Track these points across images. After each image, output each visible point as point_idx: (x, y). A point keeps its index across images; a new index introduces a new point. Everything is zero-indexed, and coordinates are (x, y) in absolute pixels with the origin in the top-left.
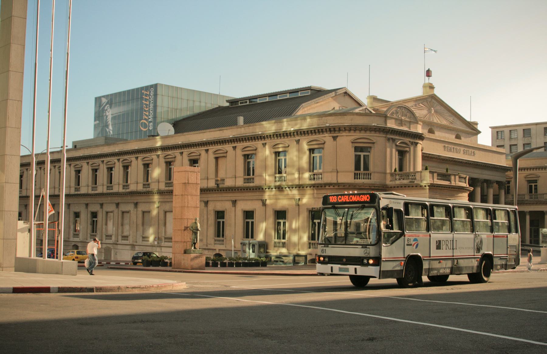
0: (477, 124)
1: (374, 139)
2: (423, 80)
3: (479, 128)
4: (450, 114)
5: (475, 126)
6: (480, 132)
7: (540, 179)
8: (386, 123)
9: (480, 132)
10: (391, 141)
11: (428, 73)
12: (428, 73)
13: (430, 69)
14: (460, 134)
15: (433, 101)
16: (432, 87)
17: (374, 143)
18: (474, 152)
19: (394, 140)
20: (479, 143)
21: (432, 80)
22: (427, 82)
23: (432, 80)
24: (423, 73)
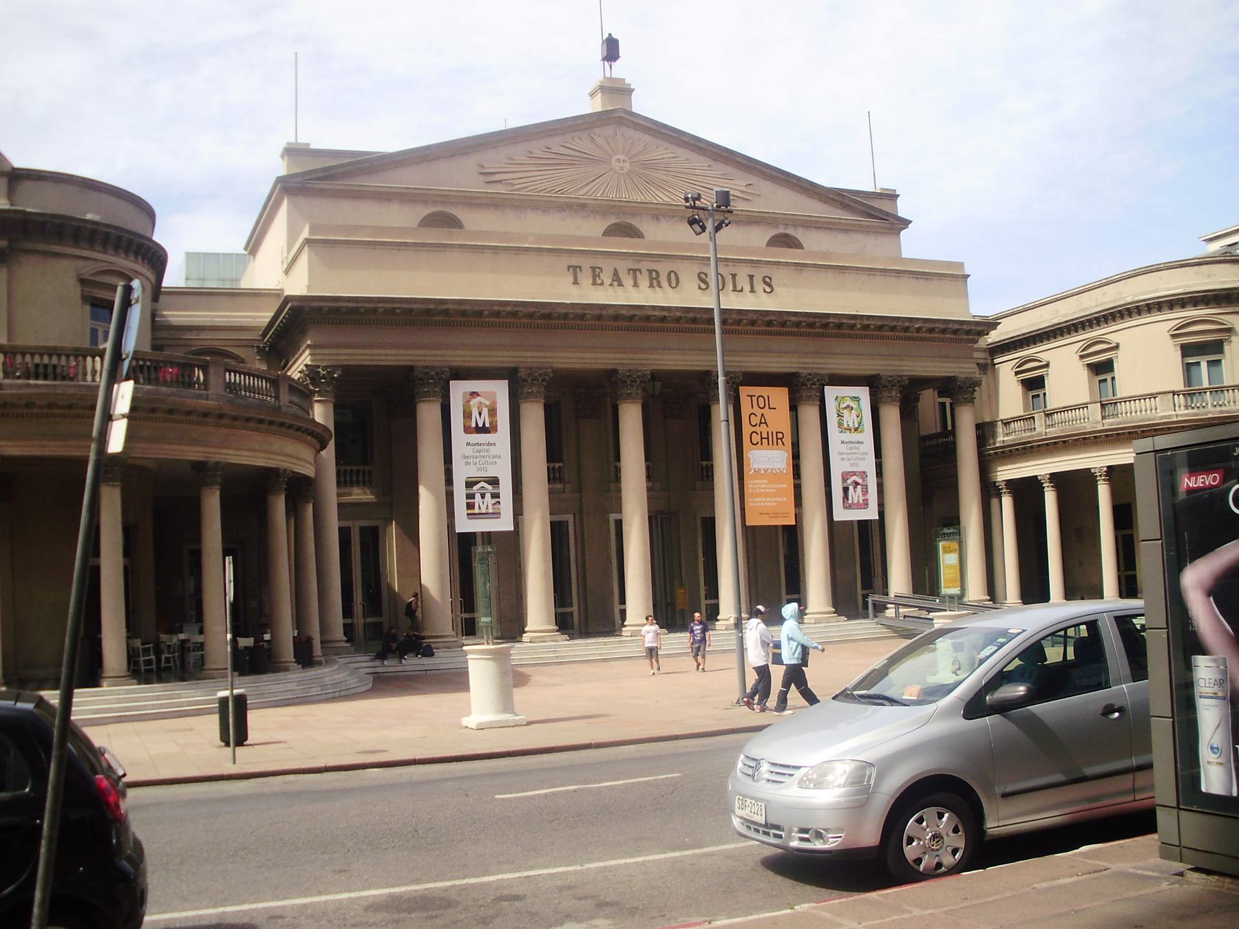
0: (892, 197)
2: (596, 71)
3: (903, 209)
4: (730, 170)
5: (884, 205)
6: (905, 223)
7: (1121, 353)
9: (905, 223)
11: (611, 50)
12: (611, 50)
13: (614, 36)
14: (799, 234)
15: (630, 133)
16: (617, 90)
18: (767, 282)
20: (907, 253)
21: (619, 70)
22: (608, 75)
23: (619, 70)
24: (597, 51)
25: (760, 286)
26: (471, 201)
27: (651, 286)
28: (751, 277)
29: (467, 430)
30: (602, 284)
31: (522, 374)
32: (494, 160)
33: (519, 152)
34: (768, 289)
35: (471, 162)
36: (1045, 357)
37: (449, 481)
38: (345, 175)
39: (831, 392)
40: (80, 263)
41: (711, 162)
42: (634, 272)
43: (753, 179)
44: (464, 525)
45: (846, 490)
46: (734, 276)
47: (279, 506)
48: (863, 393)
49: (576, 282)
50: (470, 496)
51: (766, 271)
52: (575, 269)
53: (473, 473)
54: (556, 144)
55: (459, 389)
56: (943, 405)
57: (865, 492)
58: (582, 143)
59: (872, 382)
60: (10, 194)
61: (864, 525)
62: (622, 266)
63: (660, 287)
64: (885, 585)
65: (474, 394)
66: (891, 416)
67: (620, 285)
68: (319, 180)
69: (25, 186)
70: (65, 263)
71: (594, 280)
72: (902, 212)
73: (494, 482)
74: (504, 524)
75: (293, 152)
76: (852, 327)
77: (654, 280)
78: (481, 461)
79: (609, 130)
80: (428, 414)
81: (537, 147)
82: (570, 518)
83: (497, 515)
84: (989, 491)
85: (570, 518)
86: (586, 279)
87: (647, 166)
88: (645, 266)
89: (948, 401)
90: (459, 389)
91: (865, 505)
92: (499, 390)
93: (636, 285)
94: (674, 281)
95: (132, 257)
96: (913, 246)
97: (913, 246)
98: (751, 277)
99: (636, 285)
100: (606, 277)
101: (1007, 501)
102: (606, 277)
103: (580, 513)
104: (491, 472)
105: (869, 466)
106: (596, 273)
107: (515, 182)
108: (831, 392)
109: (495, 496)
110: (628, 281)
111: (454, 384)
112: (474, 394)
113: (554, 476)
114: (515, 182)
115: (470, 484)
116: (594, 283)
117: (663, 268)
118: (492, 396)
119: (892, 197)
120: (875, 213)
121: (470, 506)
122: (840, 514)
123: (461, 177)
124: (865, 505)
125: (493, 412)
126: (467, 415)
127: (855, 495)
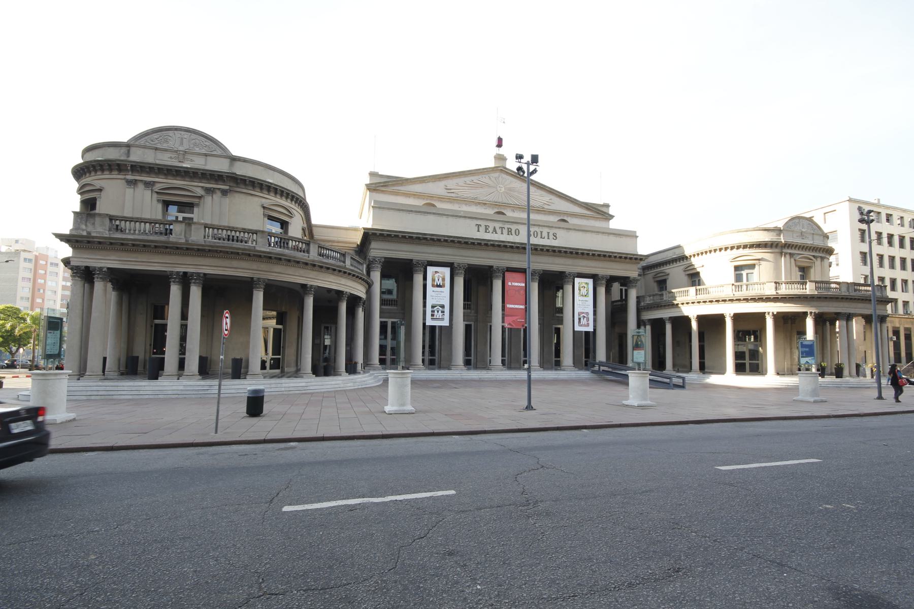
0: (607, 206)
1: (98, 184)
3: (611, 211)
5: (604, 209)
6: (612, 217)
8: (128, 154)
9: (612, 217)
10: (141, 186)
11: (500, 143)
12: (500, 143)
15: (504, 176)
16: (500, 158)
17: (100, 190)
18: (555, 235)
19: (148, 185)
23: (501, 151)
25: (551, 236)
26: (441, 199)
29: (433, 286)
31: (456, 265)
32: (451, 183)
33: (460, 181)
35: (442, 184)
36: (667, 271)
37: (425, 306)
38: (393, 185)
39: (577, 280)
40: (264, 200)
42: (502, 228)
44: (429, 322)
45: (580, 319)
47: (343, 307)
48: (590, 282)
50: (433, 311)
52: (479, 226)
53: (435, 302)
54: (475, 178)
55: (431, 270)
56: (621, 290)
57: (588, 320)
58: (485, 179)
59: (594, 277)
60: (231, 165)
61: (587, 333)
62: (498, 225)
64: (595, 357)
65: (436, 272)
66: (602, 291)
68: (381, 185)
69: (238, 164)
70: (256, 199)
72: (611, 213)
73: (443, 306)
74: (446, 323)
75: (373, 174)
76: (588, 254)
77: (510, 232)
78: (437, 297)
79: (496, 175)
80: (418, 278)
81: (468, 179)
82: (472, 323)
83: (443, 319)
84: (640, 323)
85: (472, 323)
86: (482, 229)
87: (510, 189)
88: (507, 226)
89: (624, 288)
90: (431, 270)
91: (588, 325)
92: (447, 271)
94: (517, 232)
95: (289, 200)
96: (613, 224)
97: (613, 224)
100: (491, 229)
101: (648, 328)
102: (491, 229)
103: (476, 321)
104: (441, 303)
105: (590, 310)
106: (487, 228)
108: (577, 280)
109: (443, 312)
110: (499, 231)
111: (428, 268)
112: (436, 272)
113: (466, 307)
115: (433, 307)
118: (443, 273)
119: (607, 206)
120: (601, 212)
121: (433, 315)
122: (577, 328)
123: (438, 189)
124: (588, 325)
125: (443, 279)
126: (433, 280)
127: (584, 321)
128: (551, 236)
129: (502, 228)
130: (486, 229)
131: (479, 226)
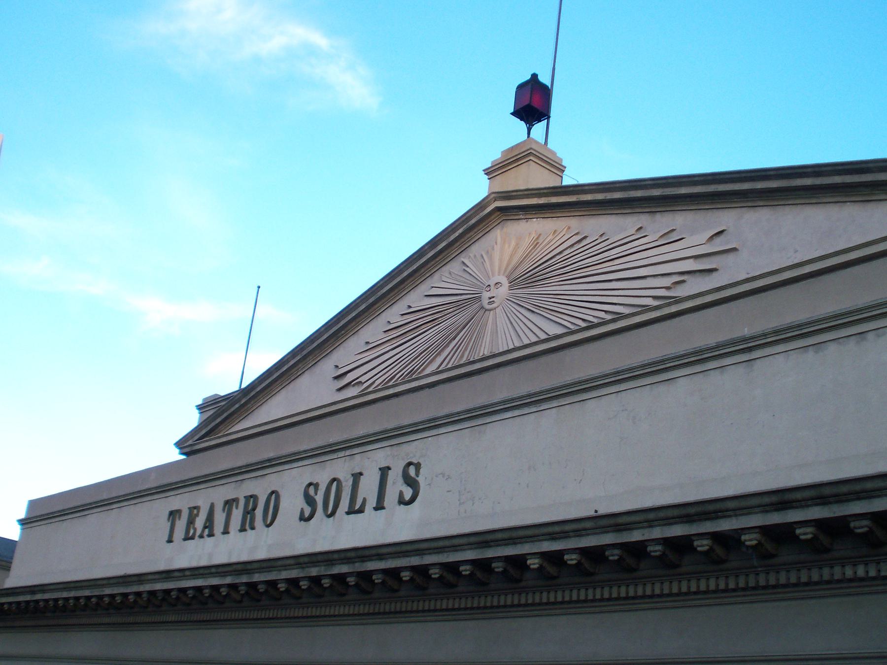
4: (676, 220)
25: (396, 486)
27: (243, 529)
28: (384, 471)
30: (192, 538)
32: (347, 354)
34: (408, 493)
35: (327, 368)
41: (643, 220)
43: (726, 218)
46: (357, 476)
49: (170, 541)
51: (413, 449)
54: (416, 299)
58: (445, 281)
63: (253, 528)
67: (211, 535)
71: (187, 531)
81: (394, 314)
93: (226, 532)
98: (384, 471)
99: (226, 532)
102: (200, 522)
107: (363, 379)
114: (363, 379)
116: (187, 538)
117: (259, 487)
128: (396, 486)
129: (229, 504)
130: (191, 522)
131: (174, 515)
